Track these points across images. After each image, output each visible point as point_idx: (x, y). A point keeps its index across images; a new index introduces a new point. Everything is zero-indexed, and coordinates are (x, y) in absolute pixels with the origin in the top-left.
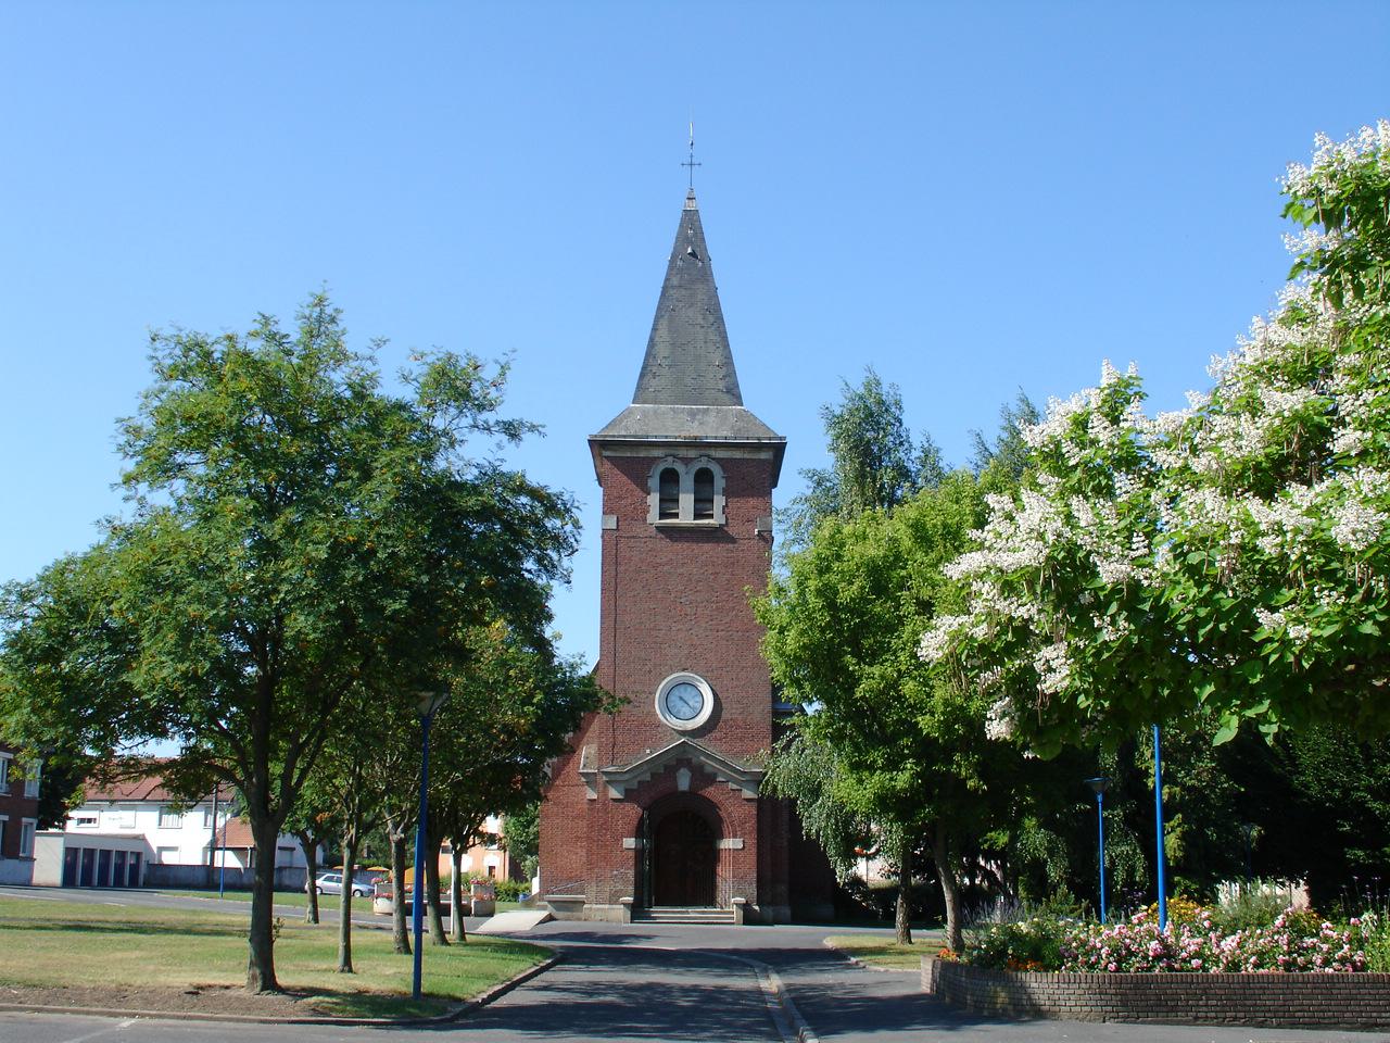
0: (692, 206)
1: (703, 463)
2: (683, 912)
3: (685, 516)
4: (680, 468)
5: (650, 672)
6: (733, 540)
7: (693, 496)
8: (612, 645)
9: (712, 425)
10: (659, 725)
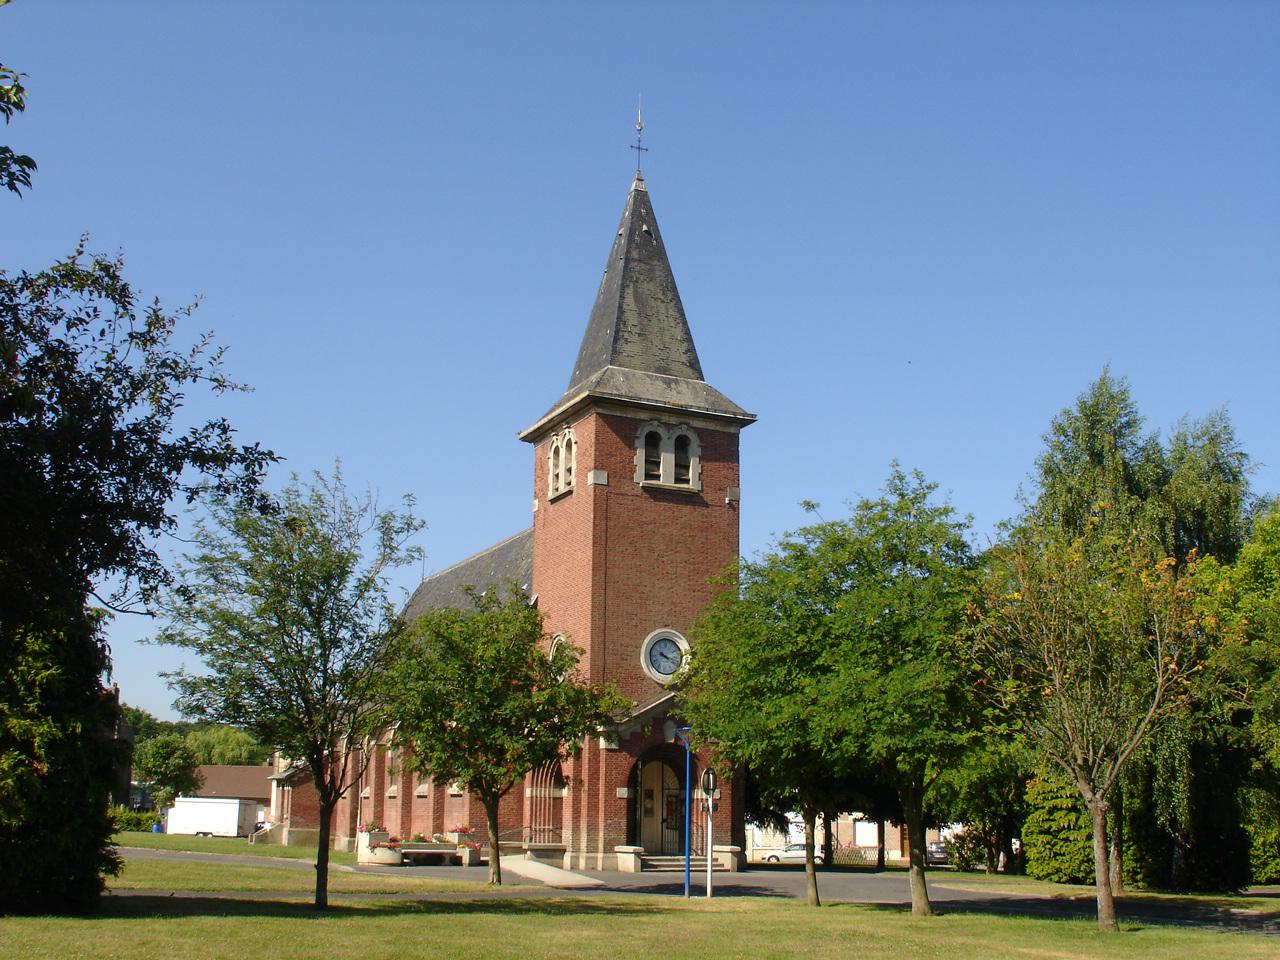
0: (643, 187)
1: (683, 431)
2: (674, 860)
3: (666, 478)
4: (662, 431)
5: (636, 626)
6: (707, 505)
7: (674, 456)
8: (602, 598)
9: (682, 395)
10: (643, 678)
